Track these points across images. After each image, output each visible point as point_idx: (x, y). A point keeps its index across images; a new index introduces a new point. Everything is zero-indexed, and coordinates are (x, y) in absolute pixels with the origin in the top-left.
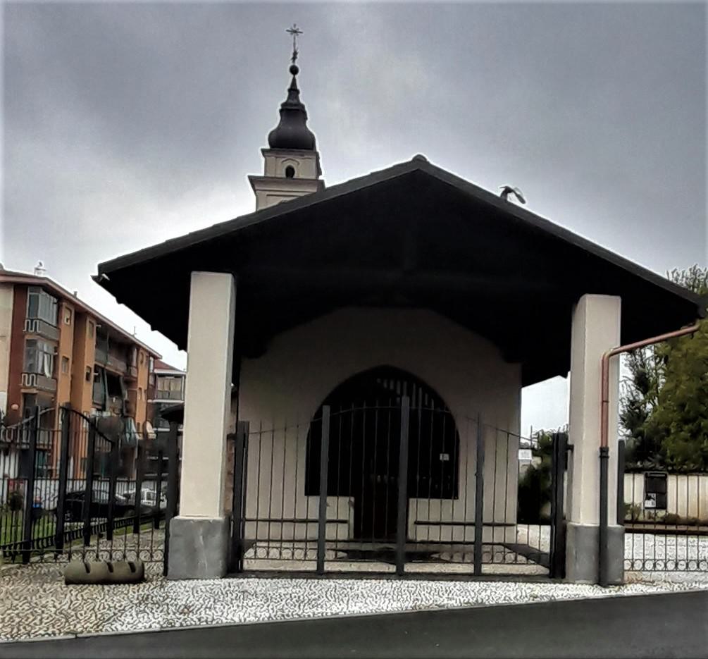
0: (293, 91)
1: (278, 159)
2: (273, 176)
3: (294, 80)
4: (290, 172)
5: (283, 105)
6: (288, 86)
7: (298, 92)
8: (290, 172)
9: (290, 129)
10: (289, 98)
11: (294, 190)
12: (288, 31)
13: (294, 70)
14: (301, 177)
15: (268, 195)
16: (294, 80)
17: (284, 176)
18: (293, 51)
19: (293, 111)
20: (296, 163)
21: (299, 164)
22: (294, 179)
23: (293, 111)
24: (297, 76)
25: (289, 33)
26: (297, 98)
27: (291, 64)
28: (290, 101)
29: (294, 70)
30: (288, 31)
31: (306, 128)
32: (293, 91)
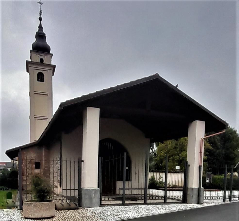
0: (40, 27)
1: (37, 55)
2: (35, 61)
3: (40, 23)
4: (42, 60)
5: (37, 33)
6: (39, 25)
7: (42, 28)
8: (42, 60)
9: (41, 43)
10: (39, 30)
11: (48, 69)
12: (43, 4)
13: (40, 19)
14: (46, 63)
15: (34, 69)
16: (40, 23)
17: (40, 62)
18: (40, 11)
19: (40, 36)
20: (44, 58)
21: (45, 57)
22: (44, 64)
23: (40, 36)
24: (41, 21)
25: (38, 3)
26: (42, 30)
27: (39, 16)
28: (40, 32)
29: (40, 19)
30: (43, 4)
31: (46, 43)
32: (40, 27)
